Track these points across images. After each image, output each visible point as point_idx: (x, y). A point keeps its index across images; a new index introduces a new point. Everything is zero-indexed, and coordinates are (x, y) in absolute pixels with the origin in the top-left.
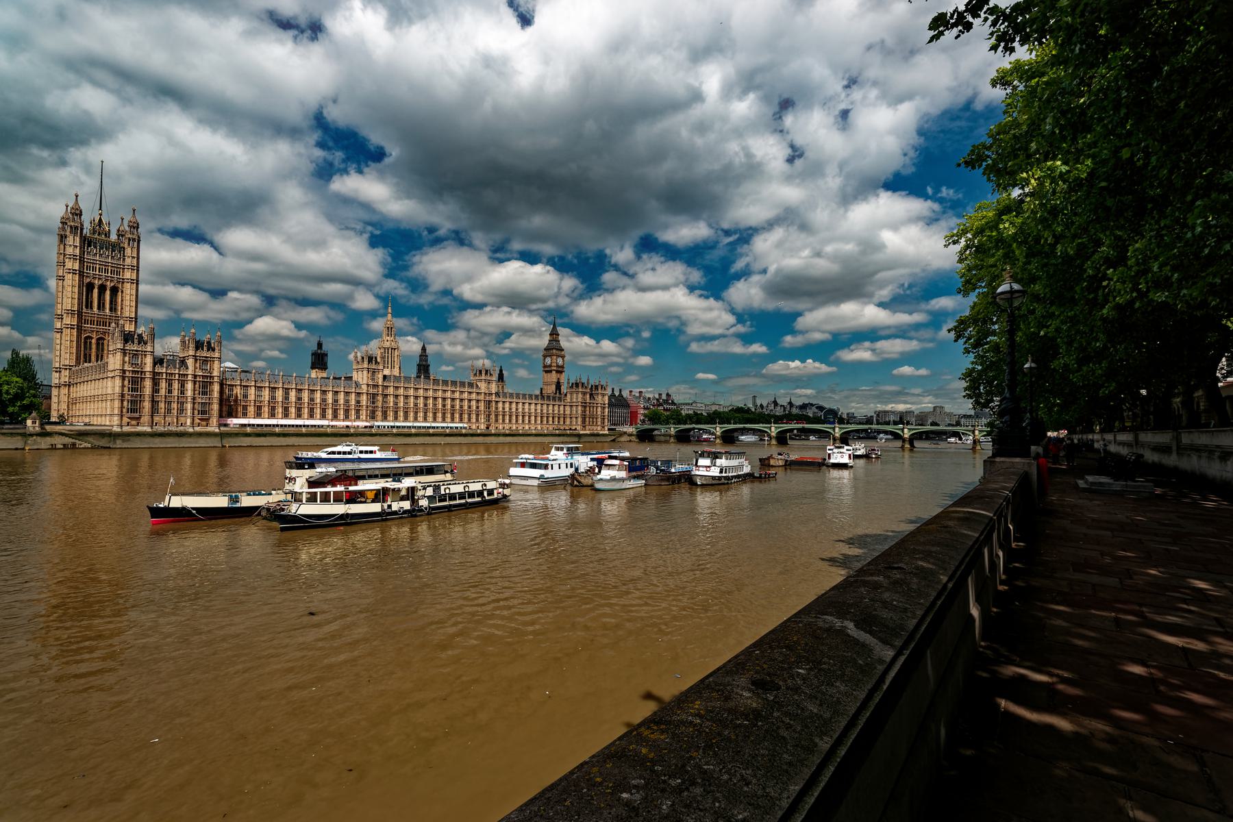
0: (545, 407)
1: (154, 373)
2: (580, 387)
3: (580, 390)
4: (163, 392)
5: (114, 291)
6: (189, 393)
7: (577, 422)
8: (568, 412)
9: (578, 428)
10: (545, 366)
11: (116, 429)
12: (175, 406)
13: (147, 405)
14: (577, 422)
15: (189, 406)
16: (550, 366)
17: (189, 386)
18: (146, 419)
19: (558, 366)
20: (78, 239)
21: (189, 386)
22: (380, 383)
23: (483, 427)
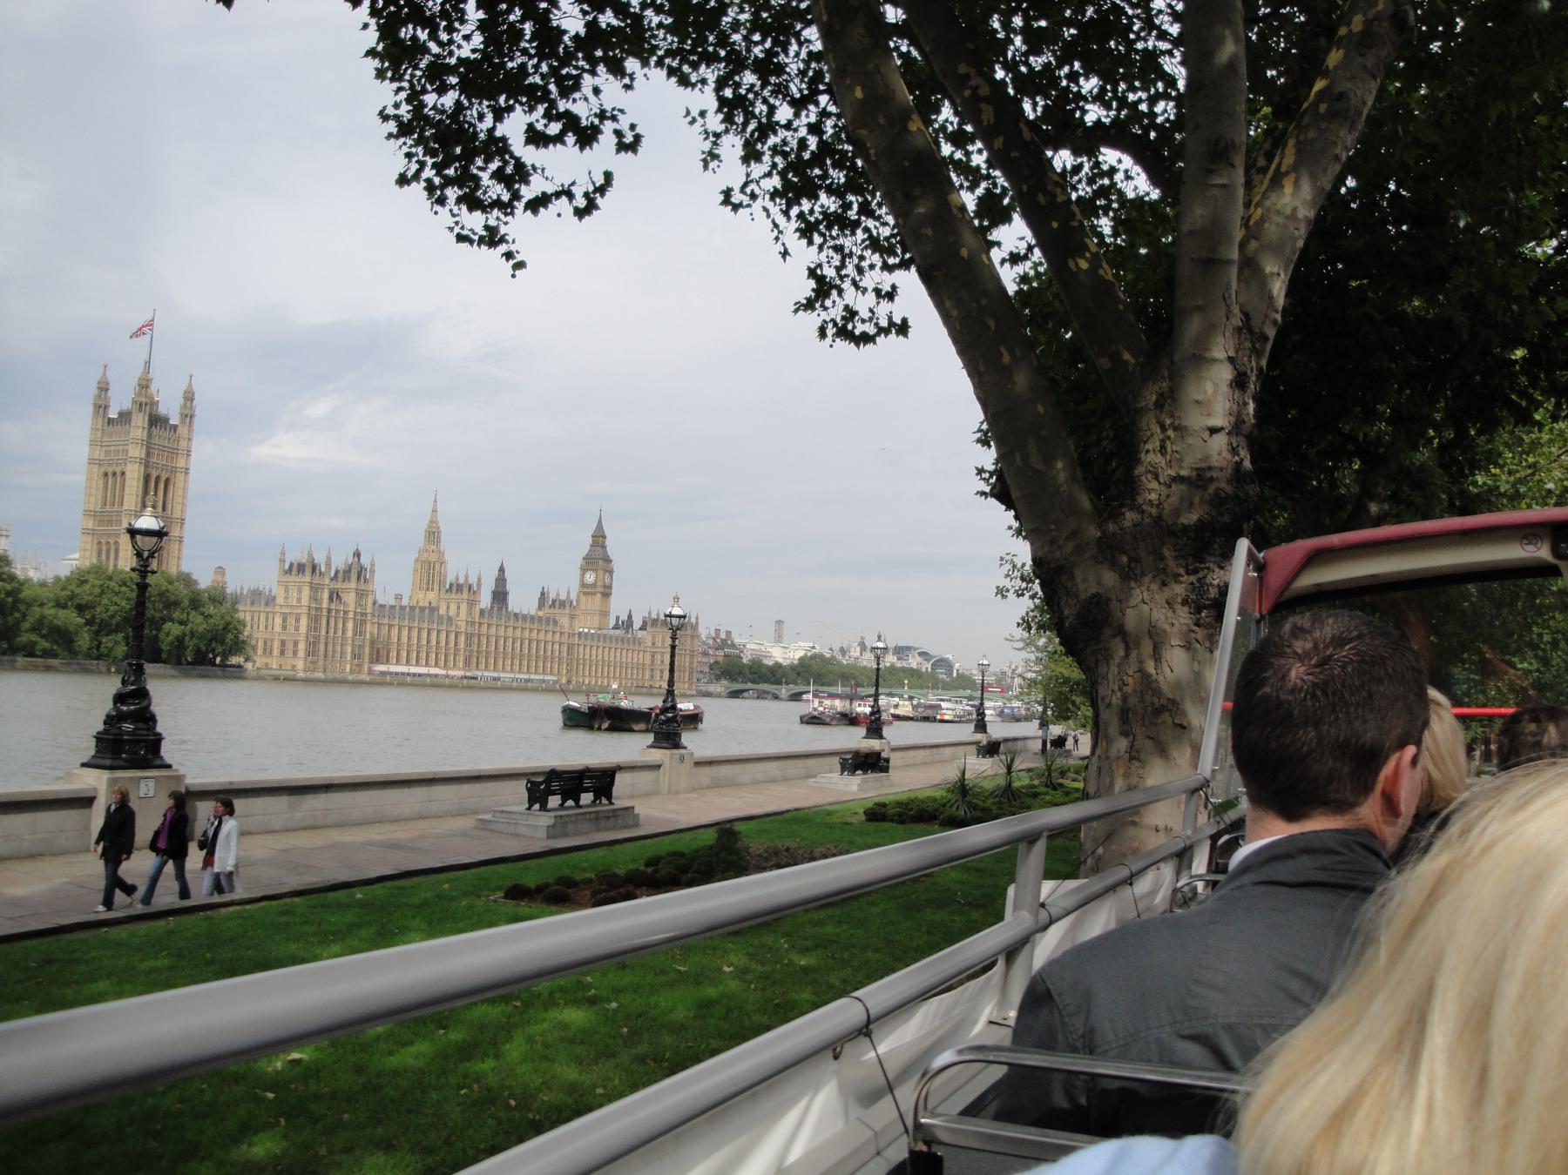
0: (624, 652)
1: (329, 611)
4: (332, 631)
5: (167, 481)
6: (350, 634)
7: (661, 677)
8: (648, 662)
10: (583, 585)
11: (301, 675)
12: (338, 648)
13: (322, 647)
14: (661, 677)
15: (349, 649)
16: (594, 585)
17: (350, 625)
18: (321, 663)
19: (605, 587)
20: (147, 419)
21: (350, 625)
22: (477, 620)
23: (564, 680)
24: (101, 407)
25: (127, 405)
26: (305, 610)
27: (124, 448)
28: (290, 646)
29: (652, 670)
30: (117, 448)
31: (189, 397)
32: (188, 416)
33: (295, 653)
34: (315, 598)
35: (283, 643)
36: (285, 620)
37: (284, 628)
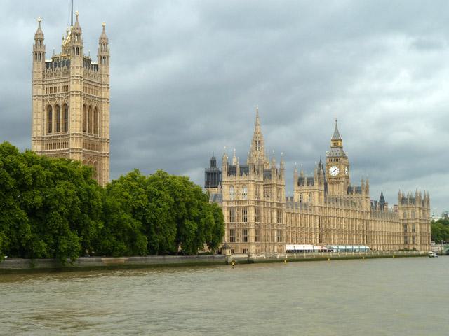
2: (417, 202)
3: (418, 205)
7: (414, 242)
9: (418, 248)
14: (414, 242)
16: (338, 177)
24: (39, 55)
25: (59, 52)
26: (252, 203)
27: (66, 84)
28: (240, 233)
29: (406, 237)
30: (57, 86)
31: (103, 43)
32: (104, 58)
33: (245, 239)
34: (257, 194)
35: (232, 232)
36: (232, 212)
37: (232, 219)
